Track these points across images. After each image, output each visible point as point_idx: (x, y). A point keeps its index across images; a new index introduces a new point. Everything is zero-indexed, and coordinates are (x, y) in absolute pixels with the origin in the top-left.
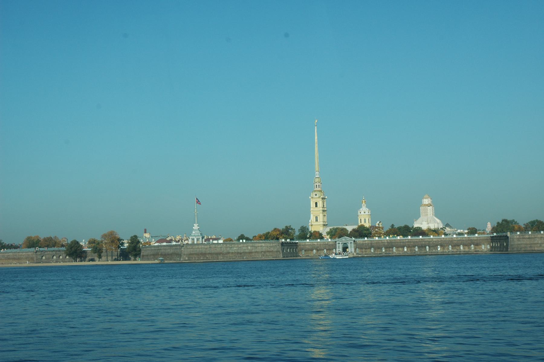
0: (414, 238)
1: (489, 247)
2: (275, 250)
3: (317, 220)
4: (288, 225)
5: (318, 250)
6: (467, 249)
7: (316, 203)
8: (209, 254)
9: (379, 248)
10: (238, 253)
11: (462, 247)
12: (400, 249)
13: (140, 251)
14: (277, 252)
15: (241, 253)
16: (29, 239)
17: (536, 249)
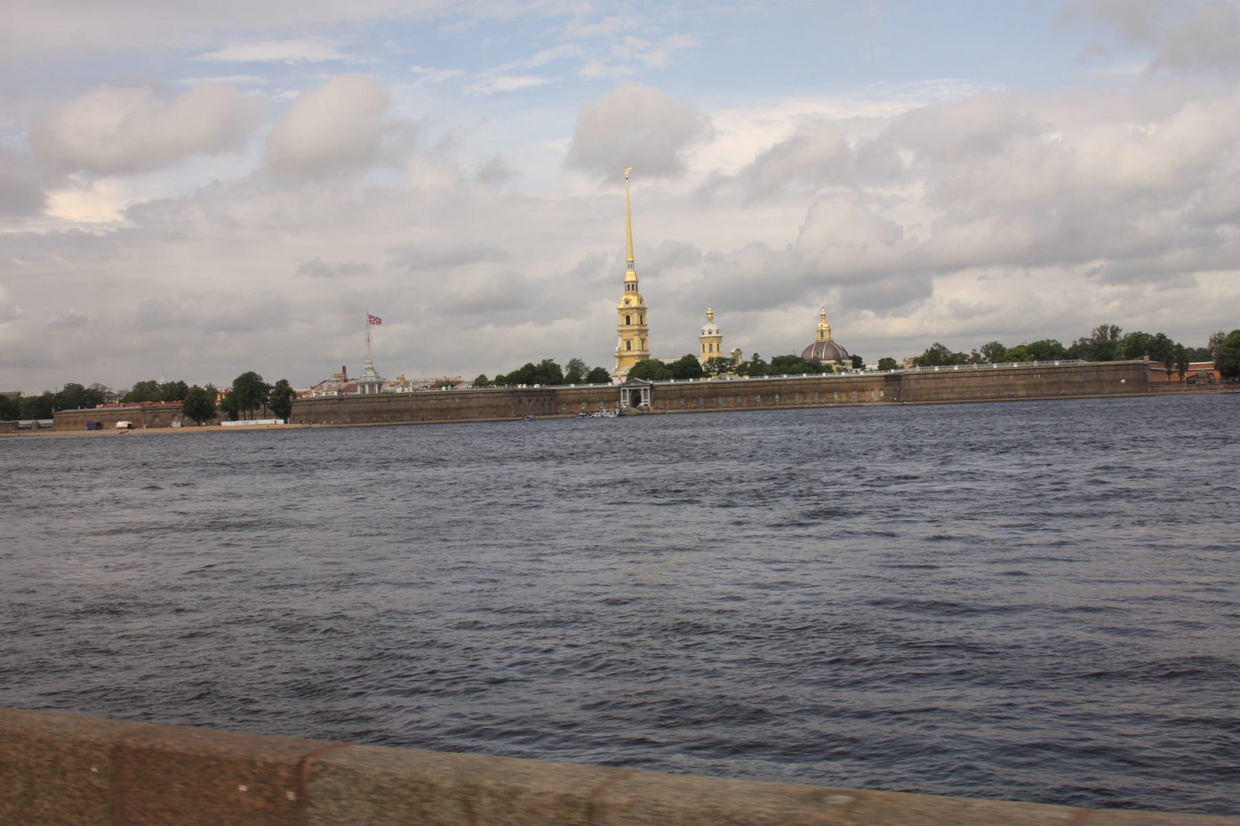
0: (773, 378)
1: (882, 394)
2: (503, 403)
3: (629, 348)
4: (547, 358)
5: (589, 403)
6: (844, 398)
7: (628, 318)
8: (388, 411)
9: (693, 398)
10: (437, 409)
11: (836, 396)
12: (731, 399)
13: (290, 408)
14: (506, 406)
15: (442, 410)
16: (141, 386)
17: (945, 396)
